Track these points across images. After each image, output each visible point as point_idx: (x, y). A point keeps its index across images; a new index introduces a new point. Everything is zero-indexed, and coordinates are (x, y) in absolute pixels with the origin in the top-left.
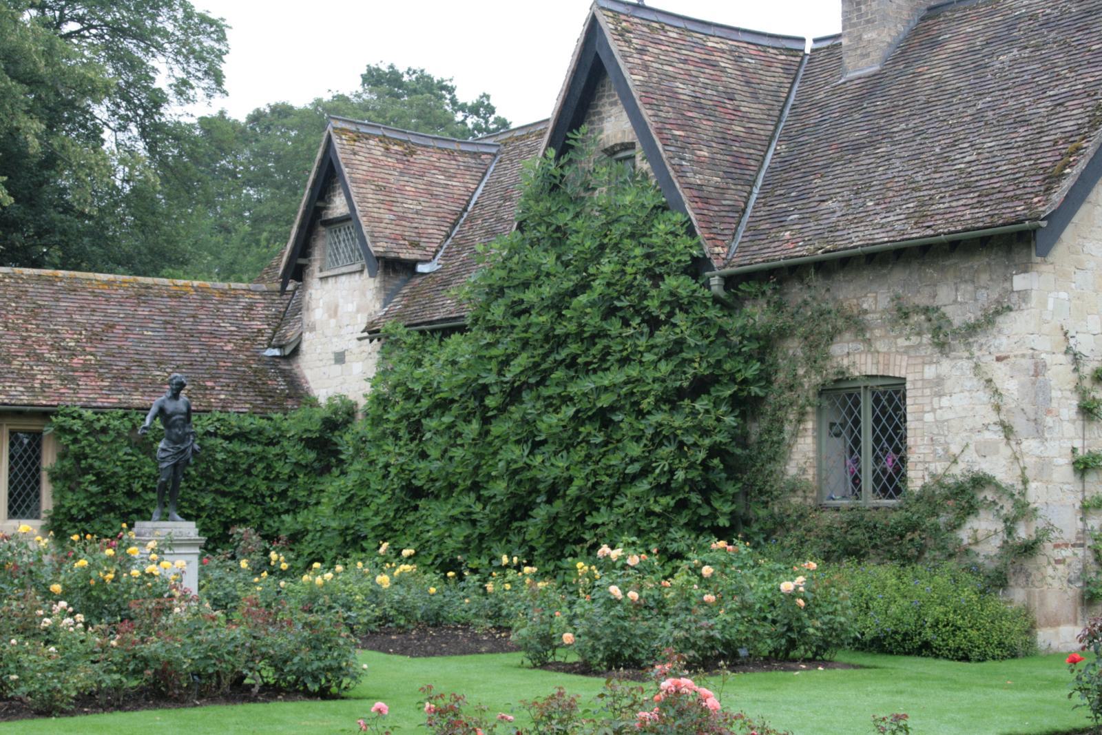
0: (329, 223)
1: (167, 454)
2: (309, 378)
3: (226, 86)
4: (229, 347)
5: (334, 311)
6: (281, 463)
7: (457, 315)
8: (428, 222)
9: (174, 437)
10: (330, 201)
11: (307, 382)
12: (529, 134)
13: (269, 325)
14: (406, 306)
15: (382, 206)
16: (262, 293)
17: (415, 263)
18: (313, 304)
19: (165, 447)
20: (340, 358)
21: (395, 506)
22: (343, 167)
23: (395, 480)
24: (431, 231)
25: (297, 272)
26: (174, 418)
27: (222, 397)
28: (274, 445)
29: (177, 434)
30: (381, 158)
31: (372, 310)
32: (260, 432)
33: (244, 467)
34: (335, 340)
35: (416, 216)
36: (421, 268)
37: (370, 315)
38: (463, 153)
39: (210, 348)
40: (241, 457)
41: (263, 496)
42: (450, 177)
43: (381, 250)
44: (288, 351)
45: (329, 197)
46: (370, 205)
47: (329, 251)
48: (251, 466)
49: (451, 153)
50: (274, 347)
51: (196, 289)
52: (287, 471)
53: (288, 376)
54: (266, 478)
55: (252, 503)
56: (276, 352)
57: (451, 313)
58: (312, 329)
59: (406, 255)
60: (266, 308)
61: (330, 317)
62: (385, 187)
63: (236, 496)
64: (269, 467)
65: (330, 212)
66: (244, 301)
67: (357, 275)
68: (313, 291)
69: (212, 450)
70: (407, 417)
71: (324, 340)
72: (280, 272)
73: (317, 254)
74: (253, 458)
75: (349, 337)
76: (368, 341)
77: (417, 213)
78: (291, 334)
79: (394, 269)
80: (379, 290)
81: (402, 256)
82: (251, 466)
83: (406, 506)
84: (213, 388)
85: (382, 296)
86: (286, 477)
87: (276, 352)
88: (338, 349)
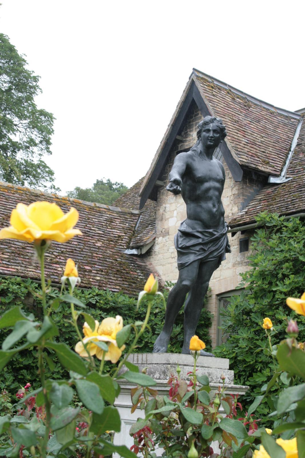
3: (51, 148)
4: (99, 244)
9: (205, 216)
10: (187, 135)
13: (125, 233)
16: (118, 213)
17: (268, 175)
18: (167, 215)
19: (189, 230)
22: (206, 102)
26: (207, 185)
27: (98, 278)
29: (210, 212)
30: (231, 103)
44: (144, 251)
49: (272, 113)
50: (132, 248)
56: (134, 252)
62: (238, 122)
66: (107, 216)
68: (167, 205)
78: (147, 239)
81: (260, 168)
84: (90, 271)
85: (241, 200)
87: (134, 252)
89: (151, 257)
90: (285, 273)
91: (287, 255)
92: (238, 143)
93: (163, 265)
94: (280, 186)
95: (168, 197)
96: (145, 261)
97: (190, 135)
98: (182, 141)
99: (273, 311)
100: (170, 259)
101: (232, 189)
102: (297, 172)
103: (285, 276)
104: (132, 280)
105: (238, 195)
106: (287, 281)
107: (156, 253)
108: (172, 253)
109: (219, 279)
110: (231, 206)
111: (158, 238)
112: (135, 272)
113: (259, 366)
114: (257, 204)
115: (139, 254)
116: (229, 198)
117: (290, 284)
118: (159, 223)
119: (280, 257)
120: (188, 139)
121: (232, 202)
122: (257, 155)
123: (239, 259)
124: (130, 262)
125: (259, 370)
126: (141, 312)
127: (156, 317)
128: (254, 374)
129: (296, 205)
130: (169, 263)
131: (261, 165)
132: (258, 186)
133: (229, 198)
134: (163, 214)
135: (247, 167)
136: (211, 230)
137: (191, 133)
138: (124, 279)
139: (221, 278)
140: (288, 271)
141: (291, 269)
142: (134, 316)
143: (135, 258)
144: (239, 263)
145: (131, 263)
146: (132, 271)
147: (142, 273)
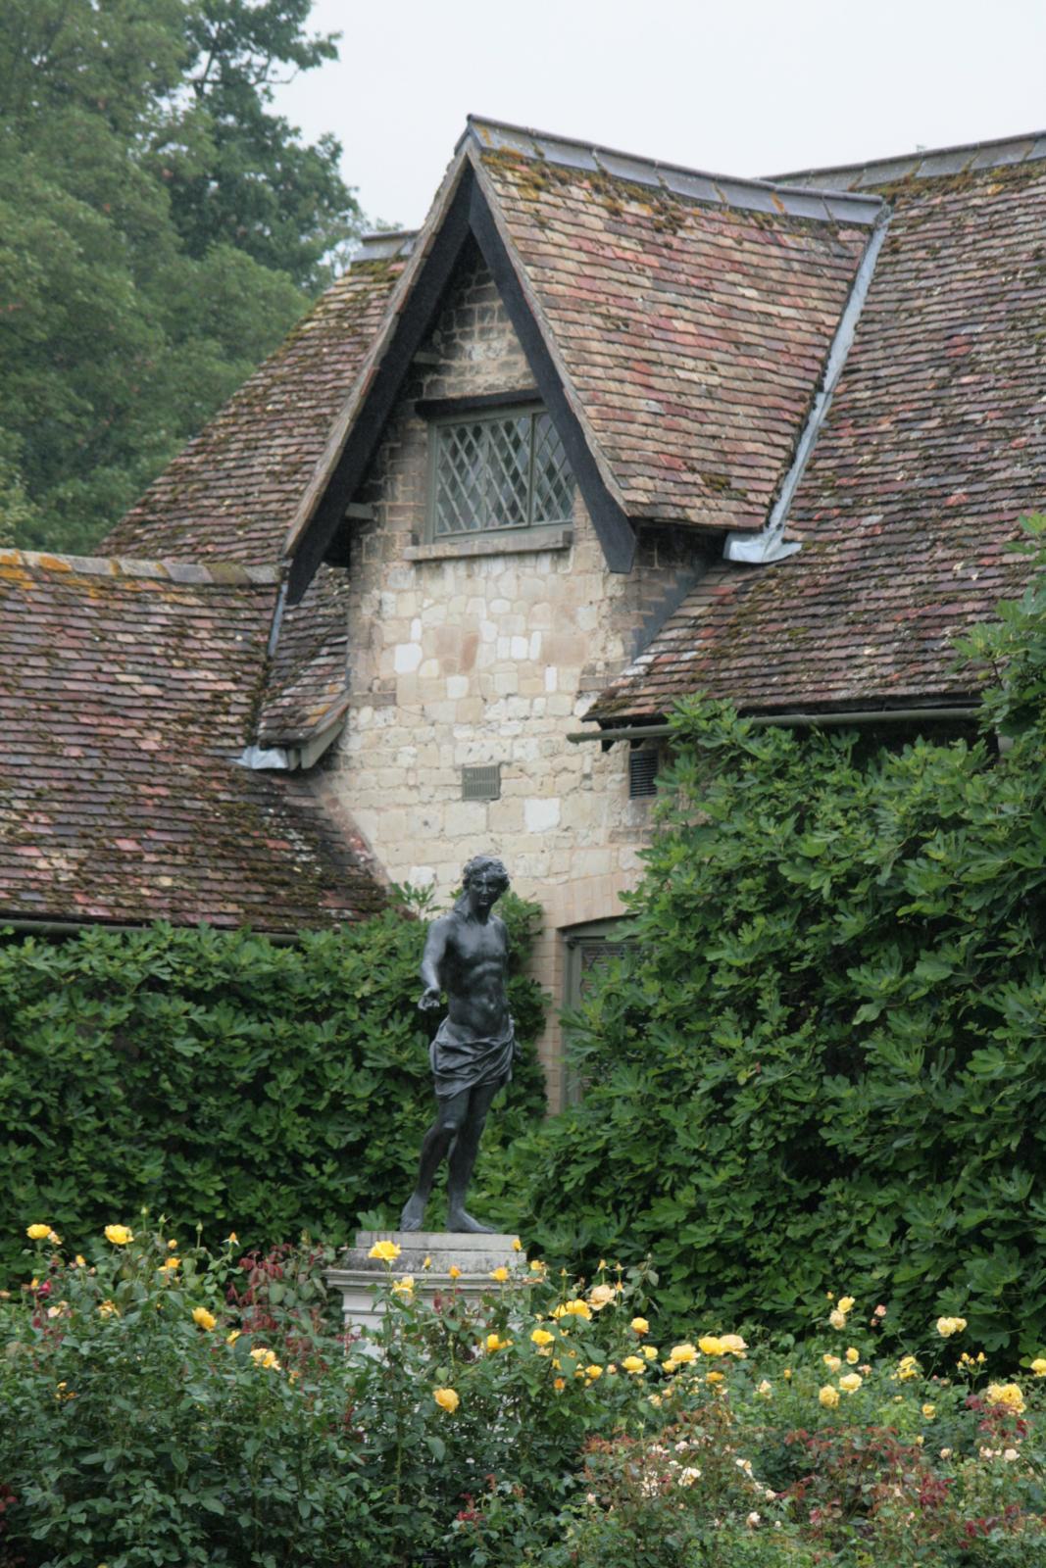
0: (440, 411)
1: (461, 1060)
2: (371, 835)
4: (151, 742)
5: (461, 653)
6: (347, 1070)
7: (912, 690)
8: (741, 421)
10: (452, 349)
11: (364, 846)
12: (968, 180)
13: (235, 681)
14: (718, 655)
15: (627, 375)
16: (202, 590)
18: (388, 631)
19: (453, 1042)
20: (481, 784)
21: (753, 1198)
22: (517, 262)
23: (756, 1126)
24: (750, 447)
25: (336, 539)
26: (479, 969)
27: (166, 882)
28: (318, 1018)
29: (484, 1011)
30: (605, 237)
31: (595, 657)
32: (278, 983)
33: (244, 1077)
34: (461, 733)
35: (708, 404)
36: (740, 550)
37: (591, 671)
38: (795, 223)
39: (105, 746)
40: (234, 1050)
41: (296, 1159)
42: (772, 293)
43: (643, 498)
44: (309, 759)
45: (448, 340)
46: (598, 372)
47: (440, 483)
48: (264, 1075)
49: (764, 223)
50: (267, 746)
51: (38, 574)
52: (362, 1093)
53: (313, 828)
54: (303, 1110)
55: (263, 1178)
56: (275, 759)
57: (891, 685)
58: (385, 697)
59: (705, 512)
60: (219, 632)
61: (448, 668)
62: (626, 322)
63: (226, 1159)
64: (312, 1080)
65: (450, 379)
66: (163, 611)
67: (546, 562)
68: (389, 597)
69: (162, 1028)
70: (781, 961)
71: (425, 732)
72: (291, 540)
73: (408, 491)
74: (265, 1054)
75: (517, 727)
76: (599, 744)
77: (710, 395)
78: (318, 712)
79: (667, 548)
80: (620, 605)
81: (694, 516)
82: (264, 1075)
83: (783, 1199)
84: (138, 858)
85: (633, 622)
86: (363, 1108)
87: (275, 759)
88: (479, 758)
89: (336, 774)
90: (745, 908)
91: (751, 853)
92: (621, 426)
93: (379, 810)
94: (762, 573)
95: (392, 565)
96: (315, 790)
97: (462, 348)
98: (435, 369)
99: (708, 1016)
100: (403, 789)
101: (605, 580)
102: (821, 520)
103: (744, 917)
104: (274, 875)
105: (625, 601)
106: (747, 936)
107: (353, 763)
108: (408, 770)
109: (565, 877)
110: (601, 635)
111: (358, 709)
112: (284, 839)
113: (668, 1179)
114: (684, 640)
115: (293, 766)
116: (595, 607)
117: (752, 943)
118: (361, 654)
119: (728, 856)
120: (455, 363)
121: (605, 622)
122: (685, 458)
123: (627, 819)
124: (261, 800)
125: (667, 1188)
126: (313, 996)
127: (363, 1010)
128: (653, 1201)
129: (791, 678)
130: (398, 805)
131: (698, 502)
132: (692, 565)
133: (595, 607)
134: (372, 625)
135: (651, 520)
136: (486, 1040)
137: (468, 345)
138: (248, 874)
139: (574, 874)
140: (753, 900)
141: (760, 895)
142: (293, 1008)
143: (277, 781)
144: (627, 833)
145: (268, 805)
146: (272, 837)
147: (307, 841)
